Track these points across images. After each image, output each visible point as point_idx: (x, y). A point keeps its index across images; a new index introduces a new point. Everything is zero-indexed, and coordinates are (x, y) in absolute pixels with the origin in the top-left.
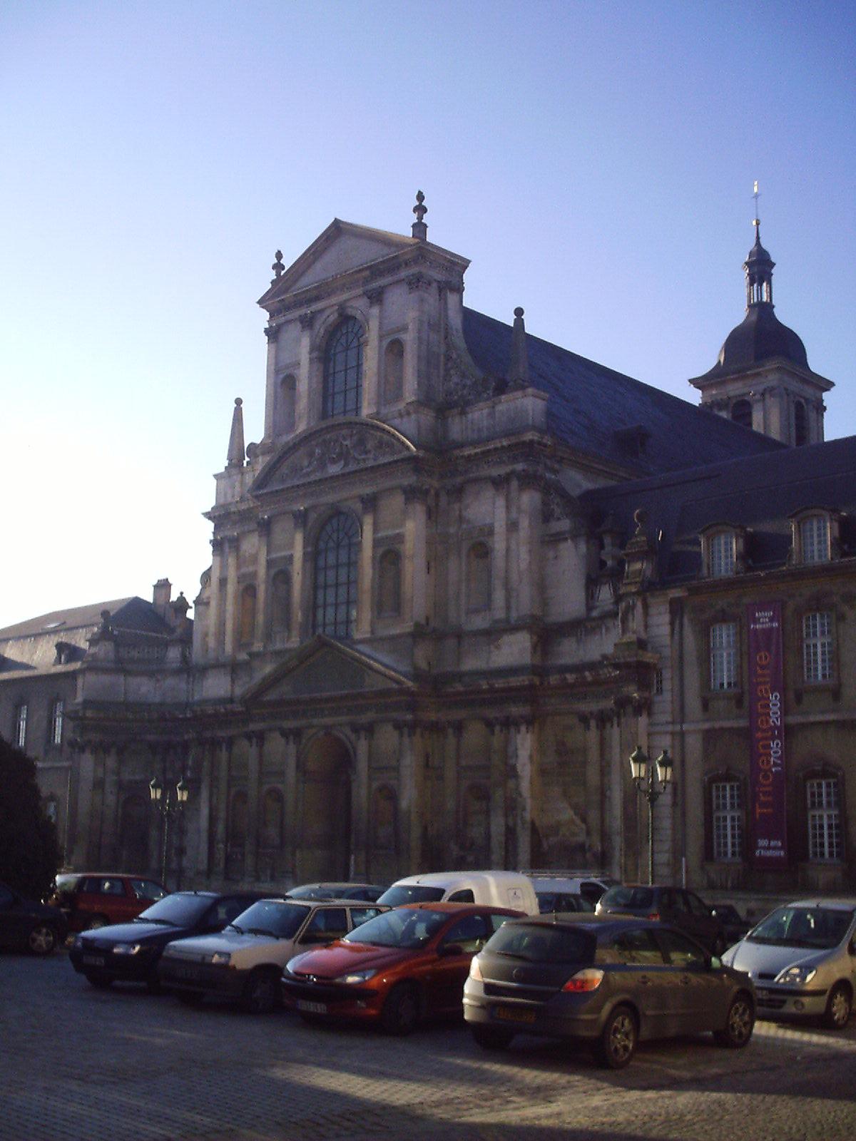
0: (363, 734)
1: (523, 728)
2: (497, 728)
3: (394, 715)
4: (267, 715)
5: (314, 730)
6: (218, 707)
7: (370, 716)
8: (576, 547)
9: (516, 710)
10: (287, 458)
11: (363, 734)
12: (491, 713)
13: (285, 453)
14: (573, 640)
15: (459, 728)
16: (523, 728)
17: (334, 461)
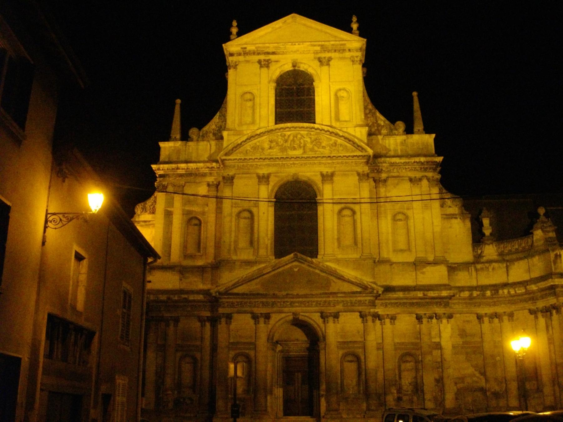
0: (331, 319)
1: (445, 321)
2: (425, 320)
3: (360, 308)
4: (236, 303)
5: (283, 315)
6: (172, 296)
7: (340, 307)
8: (464, 222)
9: (440, 310)
10: (252, 141)
11: (331, 319)
12: (421, 311)
13: (252, 137)
14: (466, 273)
15: (393, 318)
16: (445, 321)
17: (295, 149)
